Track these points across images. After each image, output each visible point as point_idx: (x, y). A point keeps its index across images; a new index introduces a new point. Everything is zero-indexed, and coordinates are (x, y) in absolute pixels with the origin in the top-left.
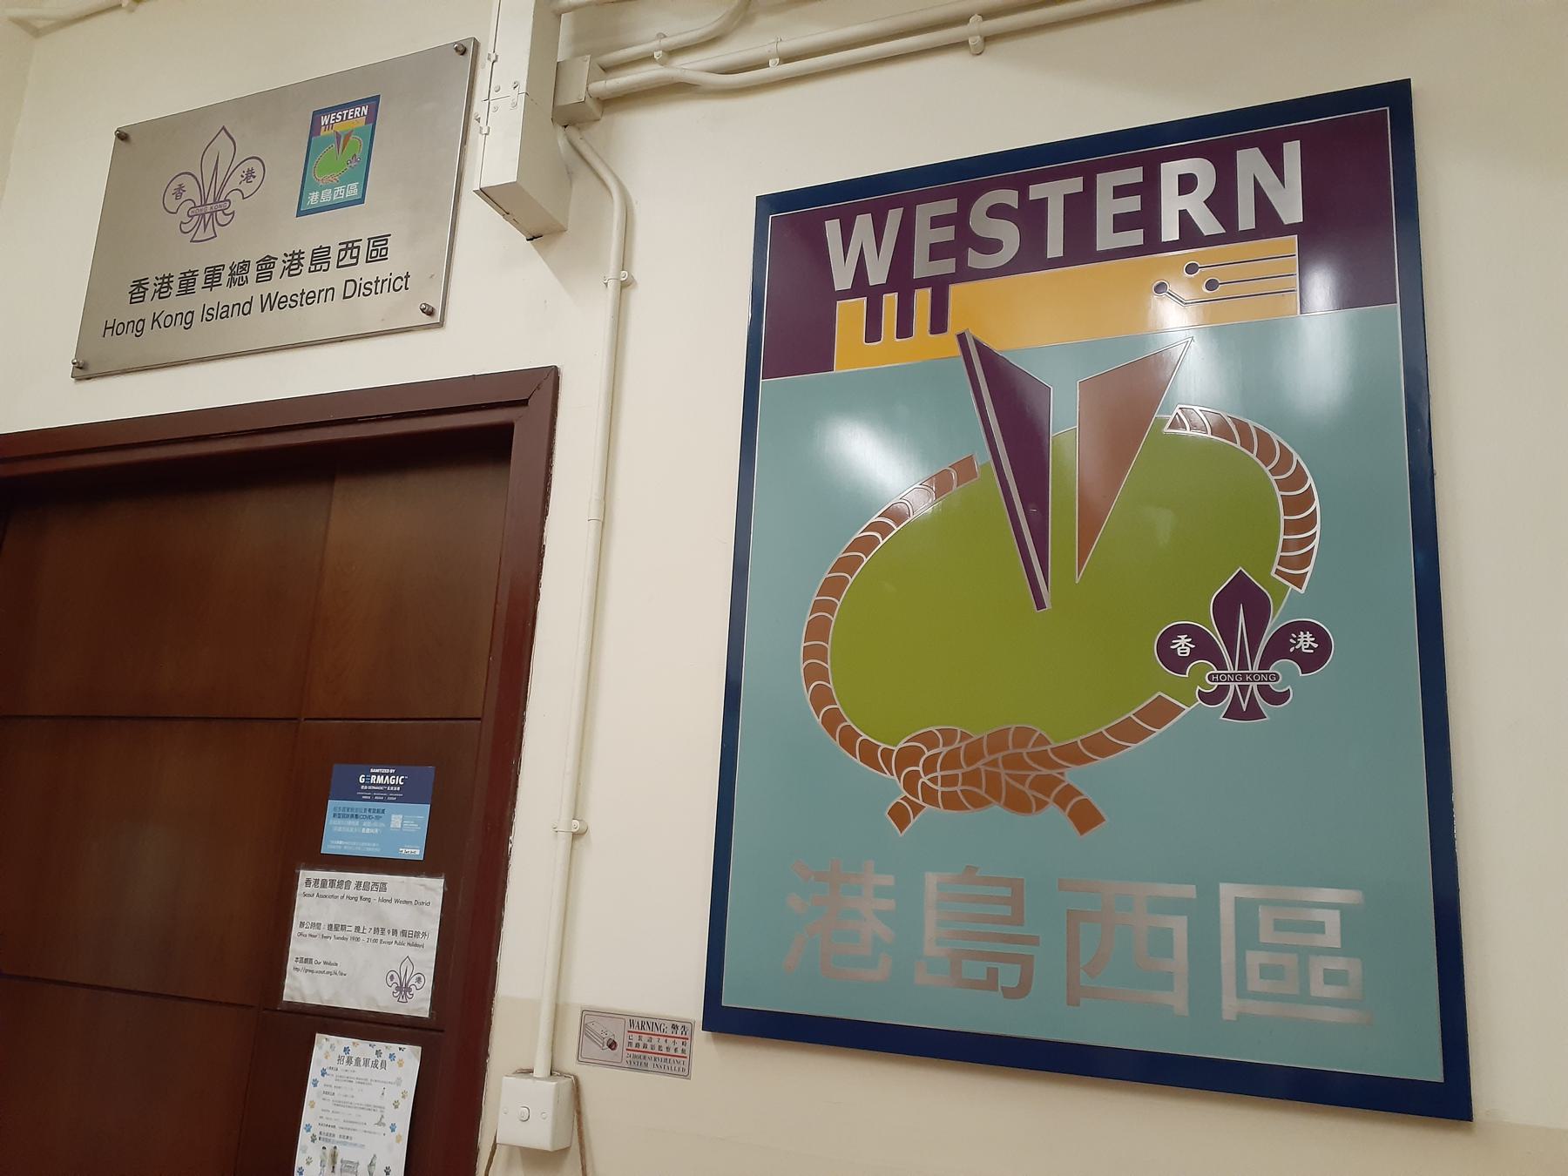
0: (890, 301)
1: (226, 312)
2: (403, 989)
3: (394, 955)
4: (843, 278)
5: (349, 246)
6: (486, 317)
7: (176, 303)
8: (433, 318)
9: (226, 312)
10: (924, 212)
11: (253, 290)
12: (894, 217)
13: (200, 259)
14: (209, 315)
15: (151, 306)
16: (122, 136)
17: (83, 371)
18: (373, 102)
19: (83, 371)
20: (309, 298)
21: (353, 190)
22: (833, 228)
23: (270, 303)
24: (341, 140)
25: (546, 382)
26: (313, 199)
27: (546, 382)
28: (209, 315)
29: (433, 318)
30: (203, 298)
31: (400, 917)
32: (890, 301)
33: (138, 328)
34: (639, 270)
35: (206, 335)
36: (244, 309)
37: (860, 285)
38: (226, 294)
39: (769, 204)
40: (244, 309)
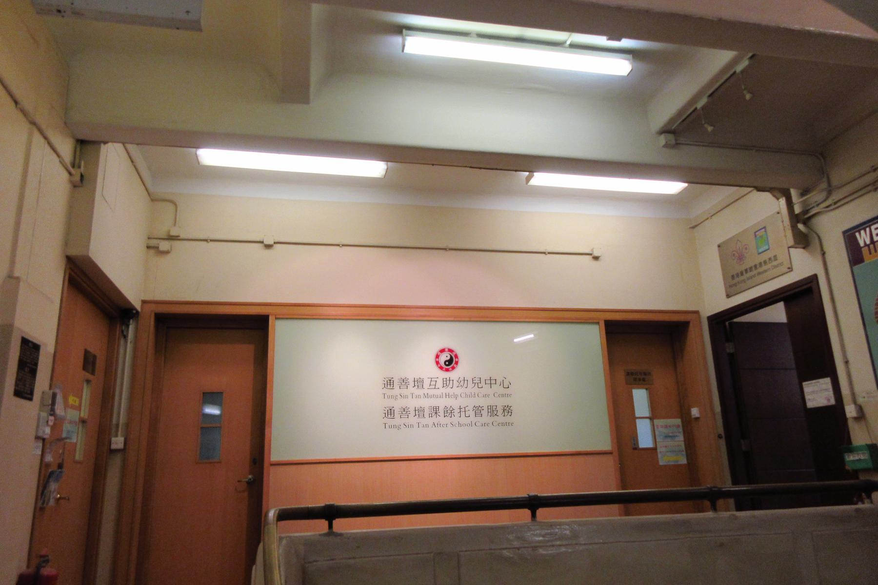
0: (872, 246)
1: (751, 278)
2: (829, 400)
3: (826, 394)
4: (862, 244)
5: (770, 259)
6: (802, 266)
7: (741, 278)
8: (790, 269)
9: (751, 278)
10: (873, 227)
11: (755, 272)
12: (868, 229)
13: (743, 268)
14: (748, 279)
15: (737, 280)
16: (719, 246)
17: (728, 296)
18: (764, 228)
19: (728, 296)
20: (765, 271)
21: (767, 247)
22: (857, 234)
23: (759, 274)
24: (761, 237)
25: (815, 278)
26: (760, 251)
27: (815, 278)
28: (748, 279)
29: (790, 269)
30: (746, 276)
31: (824, 387)
32: (872, 246)
33: (735, 285)
34: (825, 249)
35: (750, 283)
36: (754, 276)
37: (866, 245)
38: (749, 274)
39: (844, 233)
40: (754, 276)
